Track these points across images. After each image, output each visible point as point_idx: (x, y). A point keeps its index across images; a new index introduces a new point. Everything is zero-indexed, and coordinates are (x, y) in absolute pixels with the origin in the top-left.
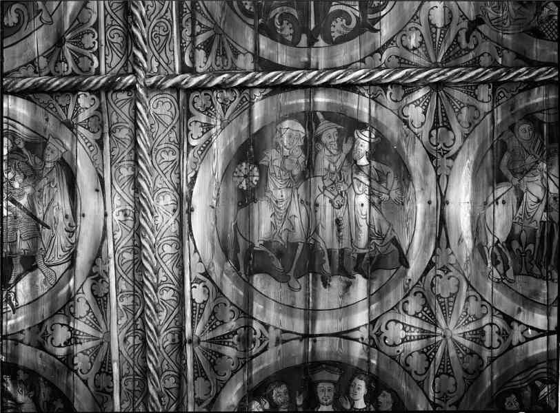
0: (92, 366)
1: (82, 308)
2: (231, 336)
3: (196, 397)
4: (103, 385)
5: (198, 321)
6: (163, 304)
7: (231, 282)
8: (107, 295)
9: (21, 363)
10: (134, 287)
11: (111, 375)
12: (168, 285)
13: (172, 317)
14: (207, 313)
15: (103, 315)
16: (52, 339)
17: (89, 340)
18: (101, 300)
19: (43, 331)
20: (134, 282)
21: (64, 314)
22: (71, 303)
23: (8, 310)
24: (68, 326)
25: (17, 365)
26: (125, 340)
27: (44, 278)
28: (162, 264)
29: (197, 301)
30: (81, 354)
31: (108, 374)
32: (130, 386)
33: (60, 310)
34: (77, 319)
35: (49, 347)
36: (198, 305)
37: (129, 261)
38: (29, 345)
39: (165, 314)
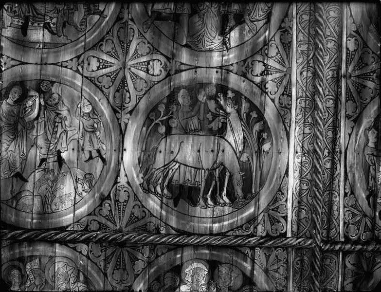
0: (278, 89)
1: (273, 52)
2: (372, 74)
3: (347, 113)
4: (285, 103)
5: (351, 63)
6: (327, 50)
7: (373, 38)
8: (291, 42)
9: (230, 86)
10: (308, 38)
11: (291, 96)
12: (331, 38)
13: (333, 60)
14: (356, 58)
15: (287, 55)
16: (252, 70)
17: (277, 72)
18: (286, 46)
19: (246, 65)
20: (309, 35)
21: (261, 54)
22: (266, 47)
23: (224, 49)
24: (263, 62)
25: (228, 87)
26: (301, 73)
27: (248, 29)
28: (328, 23)
29: (350, 49)
30: (271, 82)
31: (288, 96)
32: (303, 105)
33: (258, 52)
34: (270, 58)
35: (249, 76)
36: (351, 52)
37: (307, 20)
38: (236, 74)
39: (328, 57)
